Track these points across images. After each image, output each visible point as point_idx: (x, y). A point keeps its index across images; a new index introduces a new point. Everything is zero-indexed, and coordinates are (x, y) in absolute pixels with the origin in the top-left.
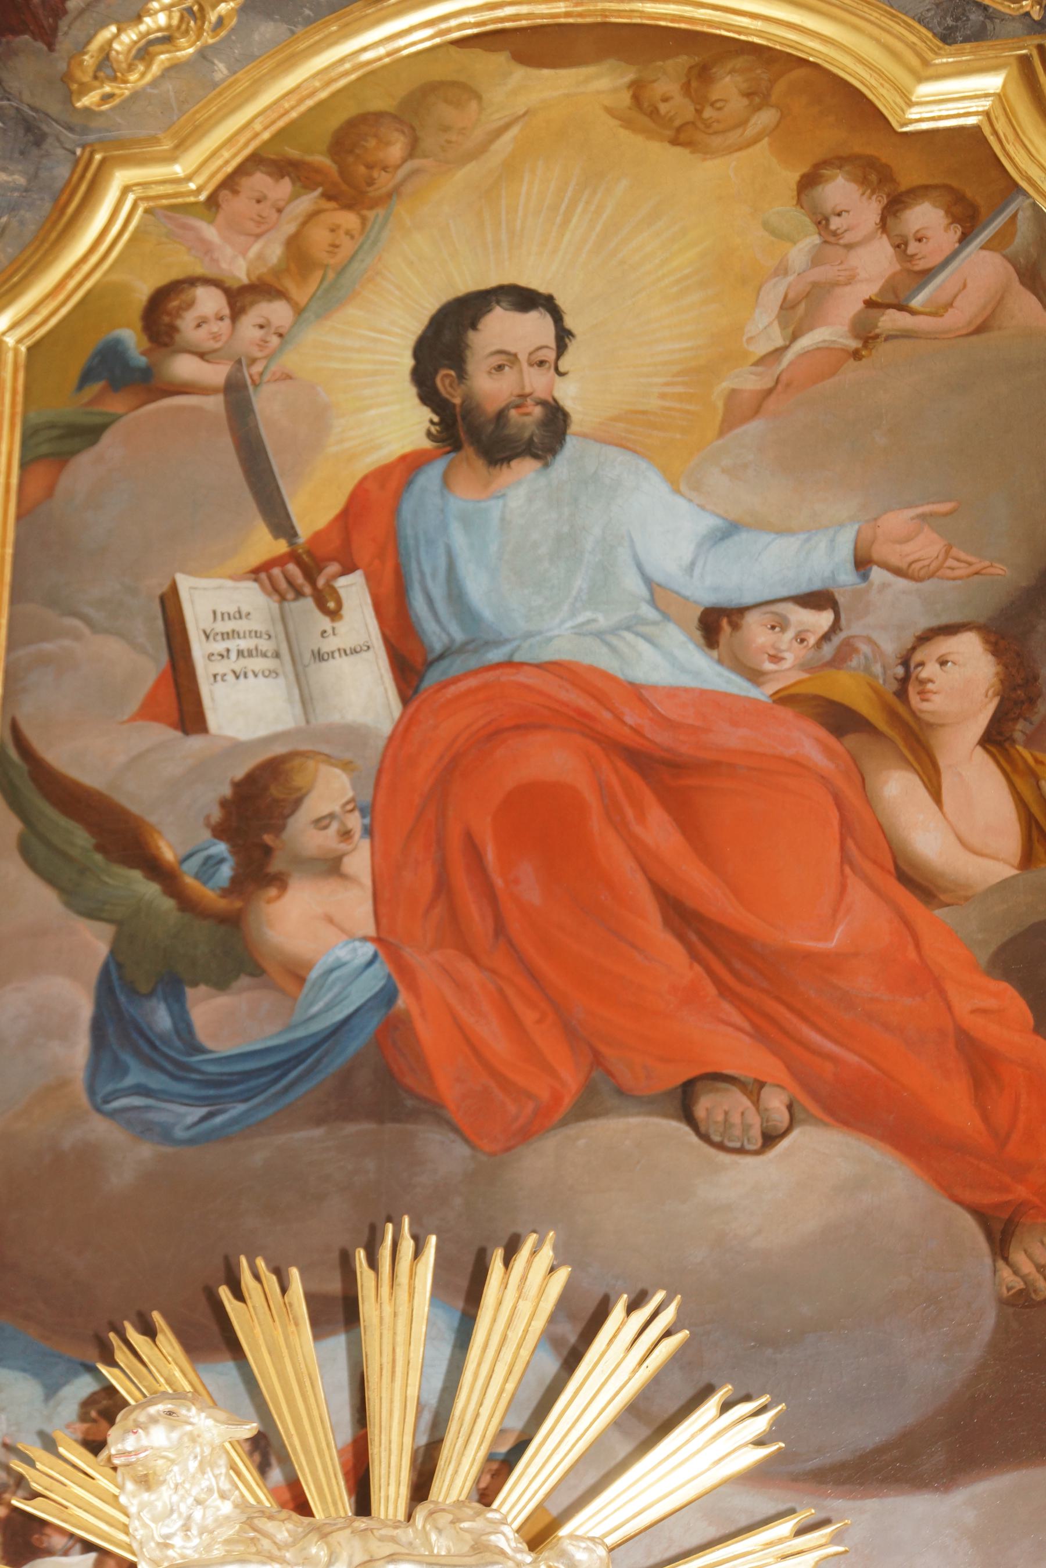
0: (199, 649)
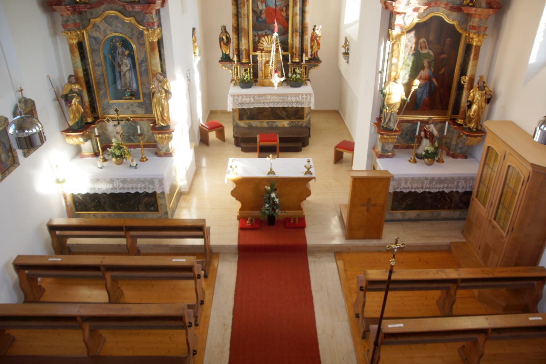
0: (259, 5)
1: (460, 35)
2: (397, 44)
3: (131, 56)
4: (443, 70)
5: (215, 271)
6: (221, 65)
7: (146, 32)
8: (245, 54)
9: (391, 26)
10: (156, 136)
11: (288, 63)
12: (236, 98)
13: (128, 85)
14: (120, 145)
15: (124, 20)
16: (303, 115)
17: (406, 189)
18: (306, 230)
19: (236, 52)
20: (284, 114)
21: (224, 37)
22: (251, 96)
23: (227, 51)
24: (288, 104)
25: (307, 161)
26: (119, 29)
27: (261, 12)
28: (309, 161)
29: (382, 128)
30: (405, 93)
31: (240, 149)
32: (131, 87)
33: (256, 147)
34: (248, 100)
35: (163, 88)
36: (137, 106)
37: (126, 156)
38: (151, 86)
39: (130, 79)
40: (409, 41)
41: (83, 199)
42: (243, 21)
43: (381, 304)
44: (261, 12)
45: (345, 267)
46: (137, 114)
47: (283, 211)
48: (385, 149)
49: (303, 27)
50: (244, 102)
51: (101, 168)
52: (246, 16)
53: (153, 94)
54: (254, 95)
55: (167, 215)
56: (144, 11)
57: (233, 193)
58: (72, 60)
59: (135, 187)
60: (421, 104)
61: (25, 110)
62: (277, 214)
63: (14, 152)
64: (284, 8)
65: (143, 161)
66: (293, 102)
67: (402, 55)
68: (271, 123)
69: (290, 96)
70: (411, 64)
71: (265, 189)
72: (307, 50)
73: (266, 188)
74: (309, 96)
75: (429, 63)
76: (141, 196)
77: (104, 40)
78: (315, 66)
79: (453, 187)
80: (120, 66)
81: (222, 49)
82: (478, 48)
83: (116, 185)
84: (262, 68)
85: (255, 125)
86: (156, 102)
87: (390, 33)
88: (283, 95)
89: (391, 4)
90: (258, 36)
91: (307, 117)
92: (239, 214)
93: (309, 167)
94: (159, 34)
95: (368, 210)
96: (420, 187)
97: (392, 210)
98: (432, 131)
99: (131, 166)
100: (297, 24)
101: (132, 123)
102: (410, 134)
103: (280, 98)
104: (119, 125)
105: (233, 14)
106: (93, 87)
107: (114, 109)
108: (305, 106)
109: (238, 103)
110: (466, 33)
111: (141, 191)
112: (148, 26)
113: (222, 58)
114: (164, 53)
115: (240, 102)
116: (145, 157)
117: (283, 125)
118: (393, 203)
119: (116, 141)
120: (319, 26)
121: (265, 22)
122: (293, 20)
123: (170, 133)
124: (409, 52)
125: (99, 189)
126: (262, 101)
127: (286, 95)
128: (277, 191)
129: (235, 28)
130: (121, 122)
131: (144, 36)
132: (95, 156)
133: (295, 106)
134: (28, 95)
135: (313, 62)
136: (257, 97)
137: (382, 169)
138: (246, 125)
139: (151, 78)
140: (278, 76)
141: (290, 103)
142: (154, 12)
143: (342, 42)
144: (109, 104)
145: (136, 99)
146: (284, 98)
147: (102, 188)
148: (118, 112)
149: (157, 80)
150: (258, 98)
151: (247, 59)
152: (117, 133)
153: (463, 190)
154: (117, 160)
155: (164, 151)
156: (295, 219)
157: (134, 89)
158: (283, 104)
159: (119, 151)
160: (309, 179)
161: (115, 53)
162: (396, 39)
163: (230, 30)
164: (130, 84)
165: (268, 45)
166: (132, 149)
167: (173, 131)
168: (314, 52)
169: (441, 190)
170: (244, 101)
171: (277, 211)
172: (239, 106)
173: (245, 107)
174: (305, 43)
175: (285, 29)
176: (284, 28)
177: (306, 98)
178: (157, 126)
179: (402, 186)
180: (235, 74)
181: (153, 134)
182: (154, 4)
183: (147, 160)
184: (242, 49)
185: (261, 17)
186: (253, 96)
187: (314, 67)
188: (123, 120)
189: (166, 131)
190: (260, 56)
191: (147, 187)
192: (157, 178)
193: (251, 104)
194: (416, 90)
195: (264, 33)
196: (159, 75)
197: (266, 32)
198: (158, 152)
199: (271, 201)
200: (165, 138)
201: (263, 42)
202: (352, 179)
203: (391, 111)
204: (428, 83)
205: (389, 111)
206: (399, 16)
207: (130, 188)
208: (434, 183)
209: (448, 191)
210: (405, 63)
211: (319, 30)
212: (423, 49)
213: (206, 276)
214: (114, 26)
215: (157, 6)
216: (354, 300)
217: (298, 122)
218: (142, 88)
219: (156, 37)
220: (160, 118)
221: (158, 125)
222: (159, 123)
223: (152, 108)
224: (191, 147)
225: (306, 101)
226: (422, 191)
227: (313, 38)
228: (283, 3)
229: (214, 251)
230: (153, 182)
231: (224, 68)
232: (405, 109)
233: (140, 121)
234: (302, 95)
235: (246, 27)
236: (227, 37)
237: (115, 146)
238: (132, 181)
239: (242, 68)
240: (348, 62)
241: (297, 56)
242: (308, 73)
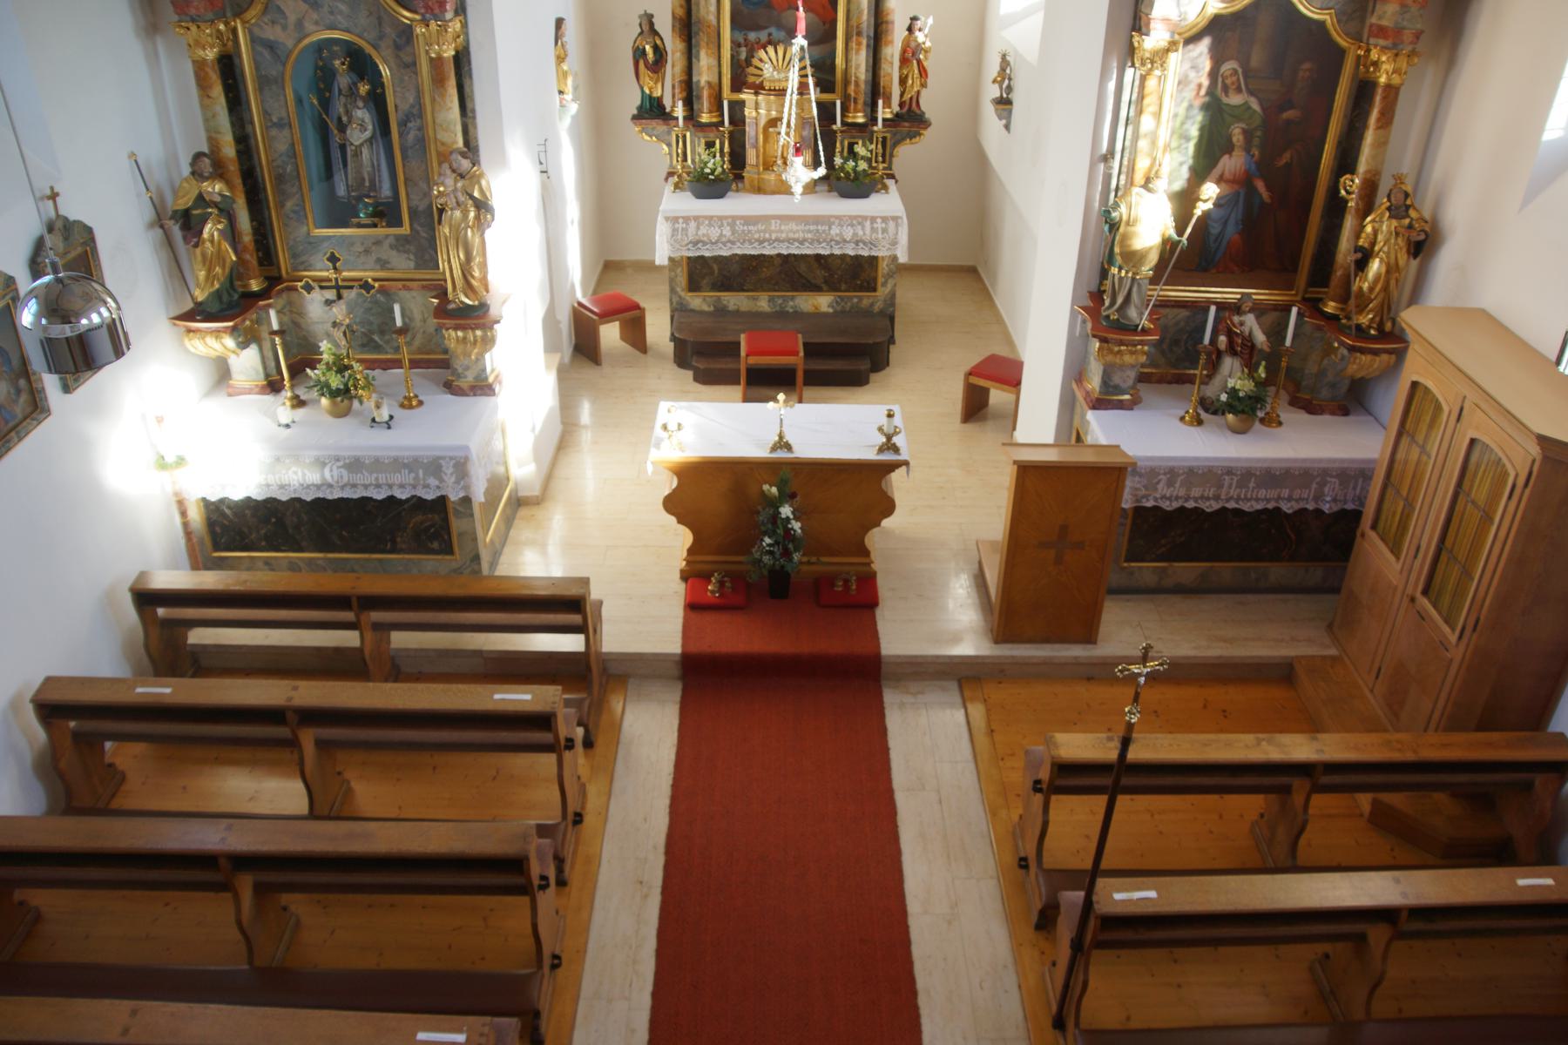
1: (1342, 53)
3: (377, 101)
4: (1286, 157)
5: (617, 727)
7: (420, 30)
8: (710, 96)
10: (449, 335)
11: (834, 127)
12: (680, 225)
13: (367, 184)
14: (342, 359)
16: (875, 279)
17: (1170, 499)
18: (879, 612)
19: (681, 93)
20: (820, 274)
22: (725, 223)
23: (656, 87)
24: (831, 247)
25: (886, 412)
29: (1104, 324)
31: (689, 374)
32: (375, 191)
33: (739, 370)
34: (714, 233)
35: (472, 197)
36: (392, 247)
38: (435, 188)
41: (235, 514)
45: (989, 721)
48: (1112, 384)
49: (880, 21)
50: (702, 239)
51: (287, 426)
53: (441, 211)
54: (734, 218)
55: (479, 564)
57: (671, 504)
58: (204, 107)
59: (384, 482)
61: (66, 254)
63: (33, 378)
65: (411, 407)
66: (845, 241)
68: (780, 301)
69: (837, 222)
72: (891, 88)
73: (766, 492)
74: (892, 224)
76: (404, 509)
77: (296, 52)
79: (1306, 496)
80: (342, 128)
81: (641, 83)
82: (1392, 91)
83: (332, 476)
84: (757, 139)
86: (448, 234)
87: (1136, 44)
88: (817, 220)
91: (884, 284)
92: (687, 564)
93: (892, 431)
94: (459, 37)
96: (1211, 496)
97: (1127, 560)
99: (373, 420)
100: (861, 13)
101: (378, 295)
103: (807, 227)
104: (342, 301)
106: (265, 189)
107: (325, 254)
109: (686, 242)
110: (1360, 47)
111: (402, 495)
112: (427, 12)
113: (640, 108)
114: (472, 91)
116: (416, 396)
117: (816, 308)
118: (1130, 540)
119: (330, 349)
120: (927, 18)
125: (282, 487)
126: (756, 236)
128: (798, 498)
129: (681, 19)
130: (345, 293)
132: (269, 390)
133: (852, 253)
134: (73, 209)
135: (906, 124)
136: (740, 224)
137: (1103, 441)
138: (709, 306)
139: (435, 164)
141: (837, 243)
143: (993, 68)
144: (312, 240)
145: (389, 225)
147: (290, 485)
148: (338, 264)
150: (745, 228)
152: (335, 324)
153: (1336, 508)
154: (334, 404)
155: (470, 377)
157: (387, 198)
158: (816, 245)
160: (891, 467)
161: (329, 88)
162: (1152, 62)
163: (664, 25)
164: (372, 182)
165: (775, 73)
166: (377, 372)
167: (498, 322)
168: (909, 96)
169: (1270, 506)
170: (704, 235)
171: (796, 557)
172: (689, 249)
173: (707, 254)
175: (827, 26)
176: (824, 24)
177: (884, 231)
178: (452, 306)
179: (1160, 491)
180: (678, 155)
181: (439, 328)
183: (421, 403)
184: (699, 81)
186: (730, 220)
188: (351, 287)
189: (475, 322)
191: (422, 482)
192: (451, 458)
194: (1206, 214)
195: (763, 36)
196: (460, 158)
197: (770, 35)
198: (453, 381)
199: (778, 528)
200: (475, 342)
201: (763, 64)
202: (1016, 467)
207: (370, 485)
208: (1252, 485)
209: (1292, 507)
212: (1231, 93)
213: (588, 744)
214: (326, 9)
216: (1016, 818)
217: (861, 299)
218: (407, 194)
220: (459, 282)
221: (455, 302)
224: (548, 367)
226: (1214, 506)
230: (439, 467)
231: (648, 138)
232: (1174, 267)
233: (400, 289)
234: (873, 219)
235: (712, 18)
236: (656, 48)
237: (327, 364)
238: (377, 464)
239: (699, 138)
240: (1007, 127)
242: (892, 156)
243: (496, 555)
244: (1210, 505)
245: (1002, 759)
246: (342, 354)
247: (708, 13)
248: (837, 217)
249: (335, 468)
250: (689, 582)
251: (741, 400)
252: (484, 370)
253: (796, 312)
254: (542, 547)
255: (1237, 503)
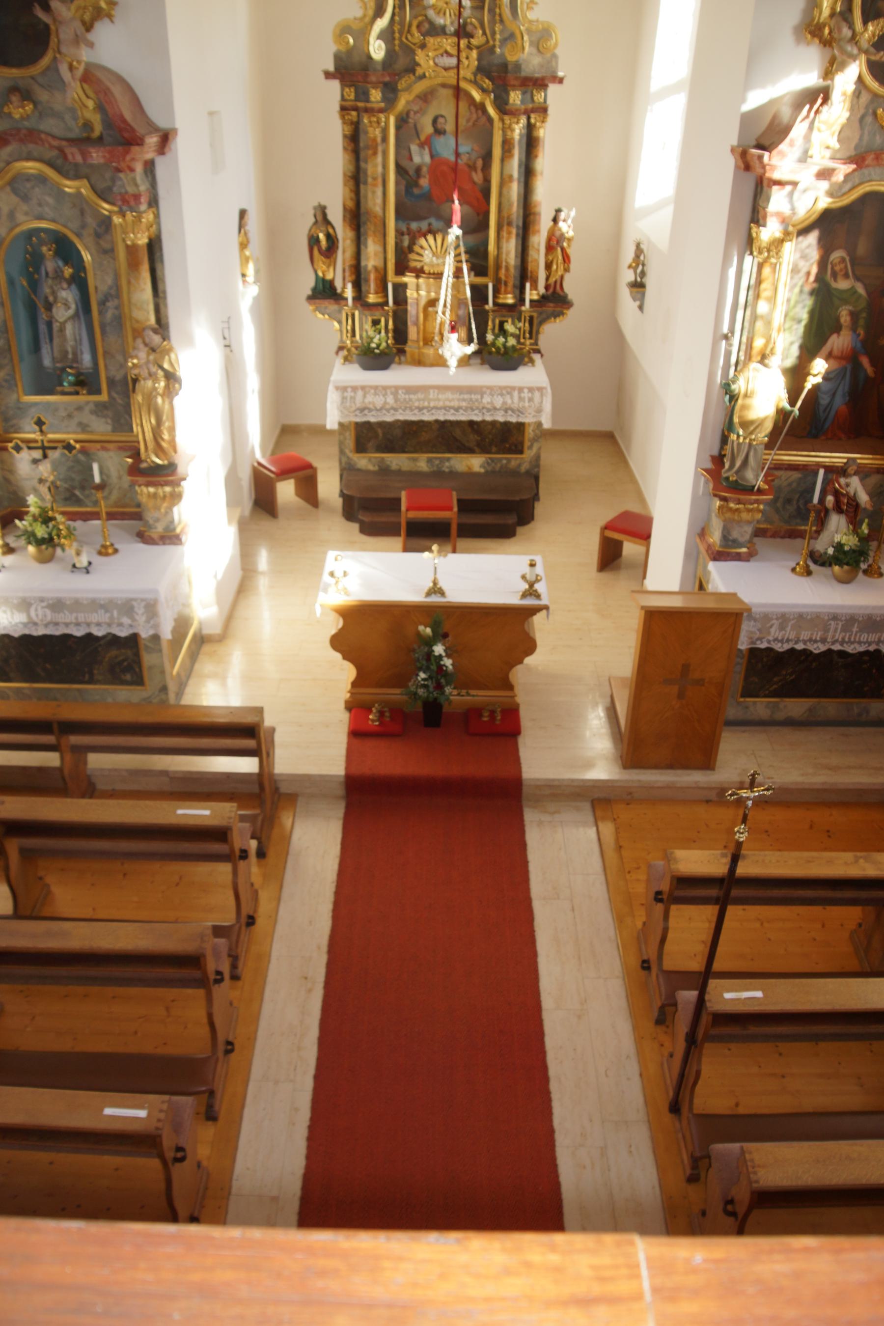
2: (771, 264)
3: (80, 281)
5: (287, 839)
6: (311, 308)
7: (117, 220)
8: (376, 279)
9: (757, 217)
10: (142, 491)
11: (487, 307)
12: (349, 394)
13: (70, 356)
14: (47, 512)
15: (62, 187)
16: (522, 443)
17: (782, 641)
19: (350, 276)
20: (472, 439)
21: (322, 236)
22: (389, 392)
23: (328, 270)
24: (483, 414)
25: (529, 562)
26: (47, 209)
27: (418, 170)
28: (532, 565)
29: (724, 484)
30: (788, 392)
31: (356, 526)
33: (399, 524)
34: (379, 401)
37: (63, 541)
38: (130, 360)
39: (75, 340)
40: (804, 257)
42: (370, 195)
43: (707, 937)
44: (418, 170)
45: (617, 840)
46: (91, 432)
47: (464, 692)
48: (731, 538)
52: (380, 180)
53: (135, 381)
54: (397, 388)
55: (167, 694)
56: (114, 164)
57: (337, 642)
59: (83, 620)
60: (826, 426)
62: (448, 699)
64: (480, 163)
65: (107, 554)
66: (495, 409)
67: (783, 294)
68: (437, 462)
69: (488, 392)
70: (805, 316)
71: (418, 634)
72: (537, 273)
73: (422, 633)
74: (537, 394)
75: (854, 315)
76: (100, 645)
78: (557, 315)
80: (49, 307)
81: (316, 267)
83: (37, 615)
85: (397, 465)
87: (754, 235)
88: (471, 390)
89: (760, 157)
90: (409, 234)
91: (530, 447)
93: (534, 579)
94: (151, 226)
95: (681, 695)
97: (742, 696)
98: (855, 494)
99: (74, 566)
102: (798, 501)
103: (462, 397)
104: (47, 461)
105: (345, 175)
108: (528, 419)
109: (353, 409)
111: (99, 632)
113: (314, 289)
114: (163, 275)
115: (358, 405)
116: (112, 545)
117: (470, 468)
118: (746, 678)
119: (36, 503)
120: (570, 210)
121: (428, 197)
122: (500, 194)
123: (177, 483)
124: (802, 286)
126: (417, 404)
127: (479, 390)
128: (450, 638)
129: (351, 211)
130: (50, 453)
131: (113, 230)
135: (551, 305)
136: (402, 393)
137: (722, 589)
138: (374, 466)
139: (130, 339)
140: (460, 340)
141: (489, 410)
142: (139, 168)
143: (628, 255)
145: (90, 393)
146: (473, 396)
148: (44, 428)
149: (146, 345)
150: (407, 397)
151: (380, 295)
152: (41, 481)
154: (40, 551)
155: (160, 528)
156: (492, 713)
157: (87, 369)
158: (469, 412)
159: (44, 526)
160: (533, 611)
161: (37, 270)
162: (769, 251)
163: (336, 216)
164: (75, 354)
165: (434, 259)
166: (78, 524)
167: (184, 479)
168: (554, 279)
169: (872, 648)
170: (370, 403)
171: (448, 690)
173: (373, 420)
174: (532, 253)
176: (478, 214)
177: (531, 400)
178: (144, 465)
180: (347, 331)
181: (133, 485)
182: (138, 144)
183: (116, 551)
184: (366, 266)
185: (417, 185)
186: (393, 390)
187: (553, 319)
188: (55, 448)
190: (414, 287)
191: (116, 621)
192: (142, 600)
193: (388, 411)
194: (816, 388)
195: (424, 225)
196: (151, 333)
197: (430, 224)
198: (145, 531)
199: (432, 664)
200: (165, 497)
202: (643, 612)
203: (751, 440)
204: (849, 367)
205: (745, 438)
206: (781, 189)
207: (71, 623)
208: (855, 629)
210: (791, 314)
211: (569, 221)
212: (839, 278)
213: (261, 854)
215: (148, 152)
216: (639, 925)
217: (509, 460)
218: (106, 366)
219: (143, 232)
220: (151, 445)
221: (147, 461)
222: (150, 458)
223: (131, 418)
224: (230, 521)
225: (530, 406)
226: (823, 648)
227: (551, 242)
228: (476, 148)
229: (284, 788)
230: (132, 608)
232: (786, 434)
233: (98, 450)
234: (521, 390)
235: (378, 210)
236: (328, 236)
237: (34, 516)
238: (77, 605)
239: (366, 317)
240: (641, 308)
241: (509, 288)
242: (538, 333)
243: (182, 686)
244: (818, 647)
245: (629, 872)
246: (46, 507)
247: (375, 205)
248: (488, 388)
249: (39, 608)
250: (353, 711)
251: (401, 550)
252: (172, 522)
253: (451, 472)
254: (222, 678)
255: (842, 644)
